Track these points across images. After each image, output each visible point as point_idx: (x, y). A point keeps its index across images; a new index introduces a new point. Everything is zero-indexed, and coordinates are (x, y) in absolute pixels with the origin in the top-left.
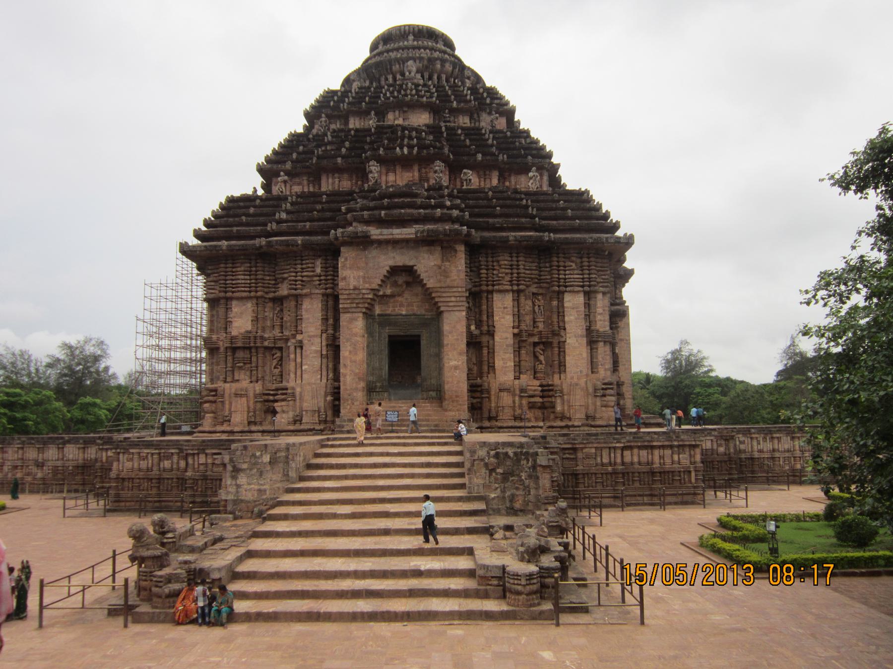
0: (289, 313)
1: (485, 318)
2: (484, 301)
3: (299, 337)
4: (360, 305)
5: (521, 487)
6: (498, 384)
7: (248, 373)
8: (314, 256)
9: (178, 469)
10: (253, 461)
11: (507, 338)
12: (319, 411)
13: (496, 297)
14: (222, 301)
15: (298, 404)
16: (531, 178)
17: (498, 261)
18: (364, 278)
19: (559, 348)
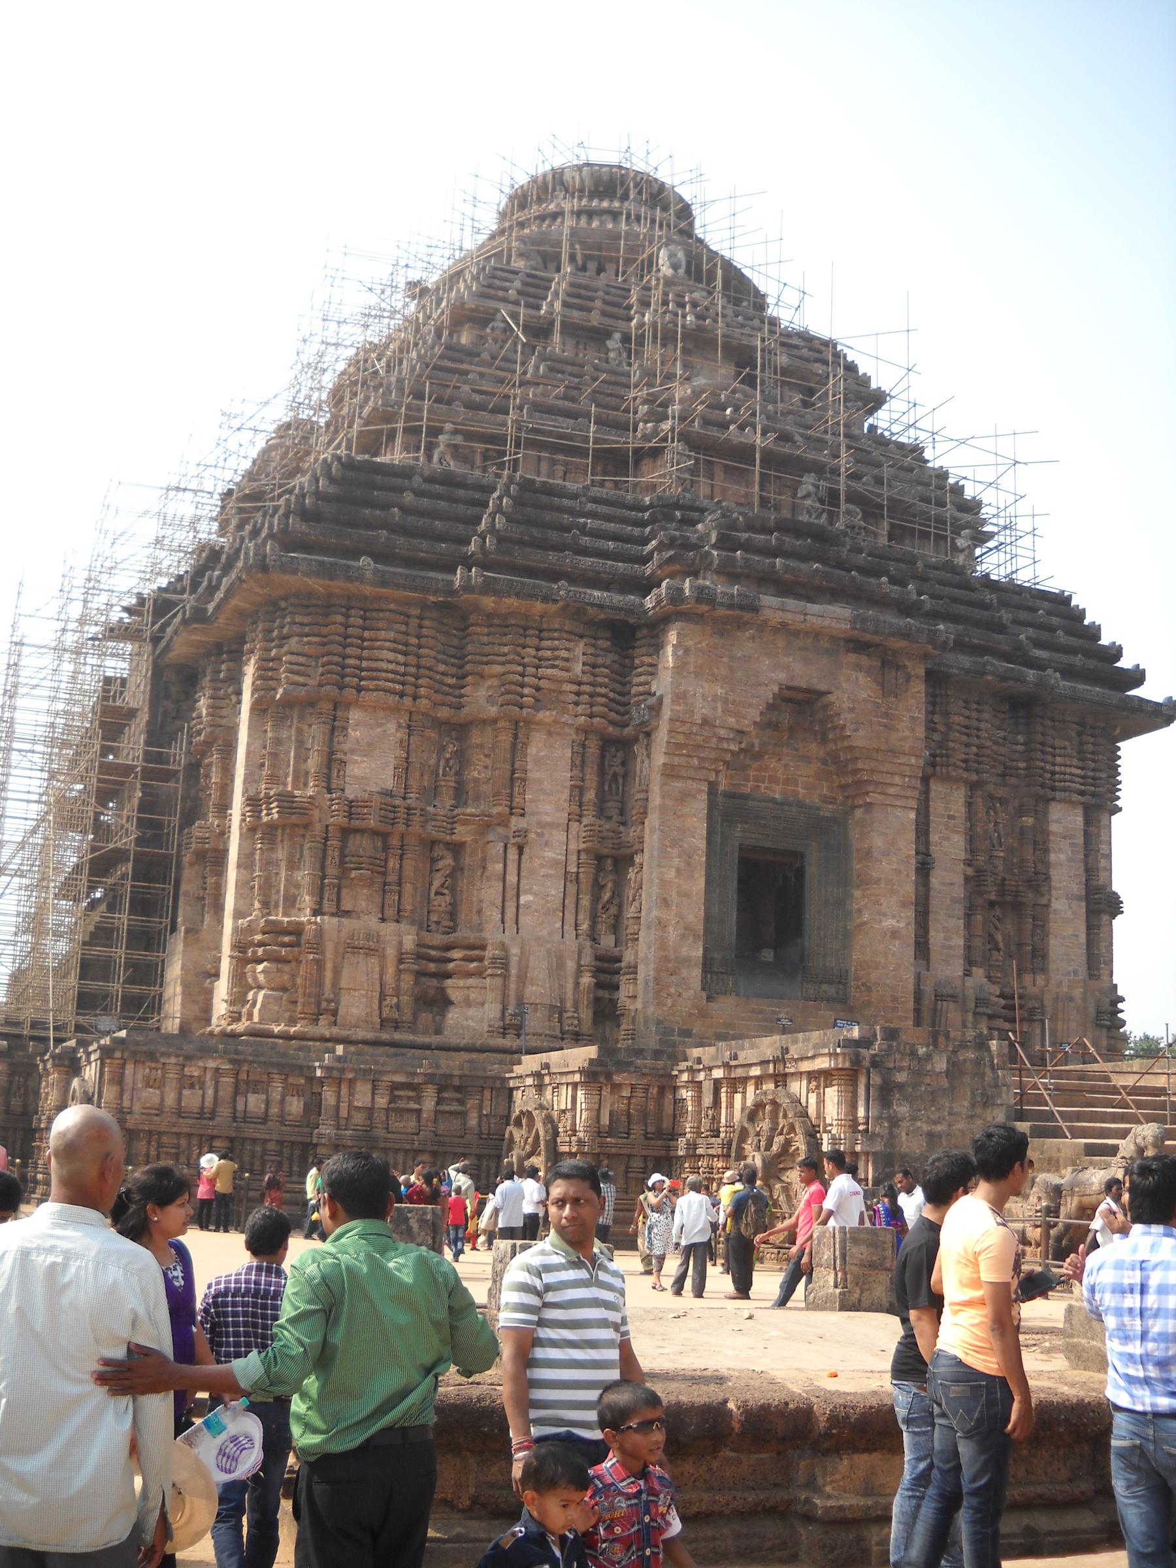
0: (488, 762)
7: (377, 898)
8: (570, 632)
9: (282, 1119)
12: (561, 1011)
13: (936, 788)
15: (513, 986)
16: (962, 551)
17: (946, 714)
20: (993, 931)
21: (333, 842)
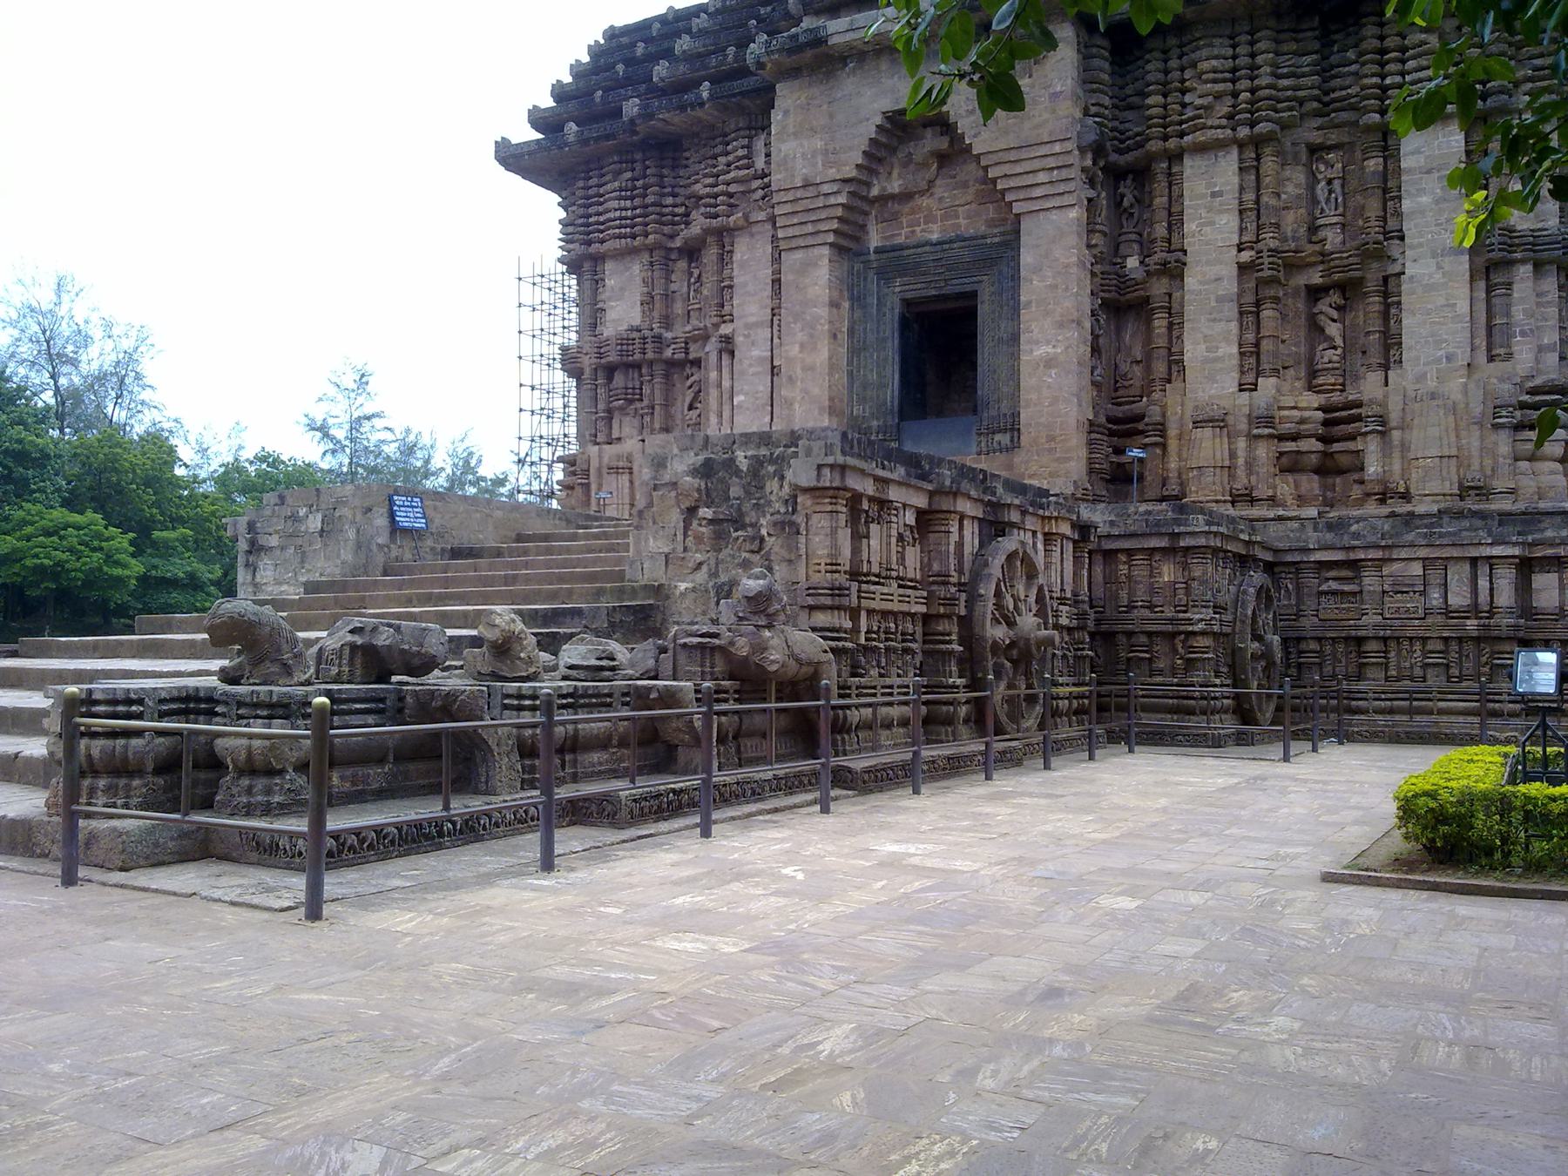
1: (1161, 230)
2: (1160, 186)
3: (725, 329)
4: (824, 227)
5: (756, 558)
6: (1190, 406)
7: (636, 422)
8: (749, 128)
11: (1216, 280)
13: (1192, 167)
14: (587, 266)
17: (1194, 65)
19: (1386, 295)
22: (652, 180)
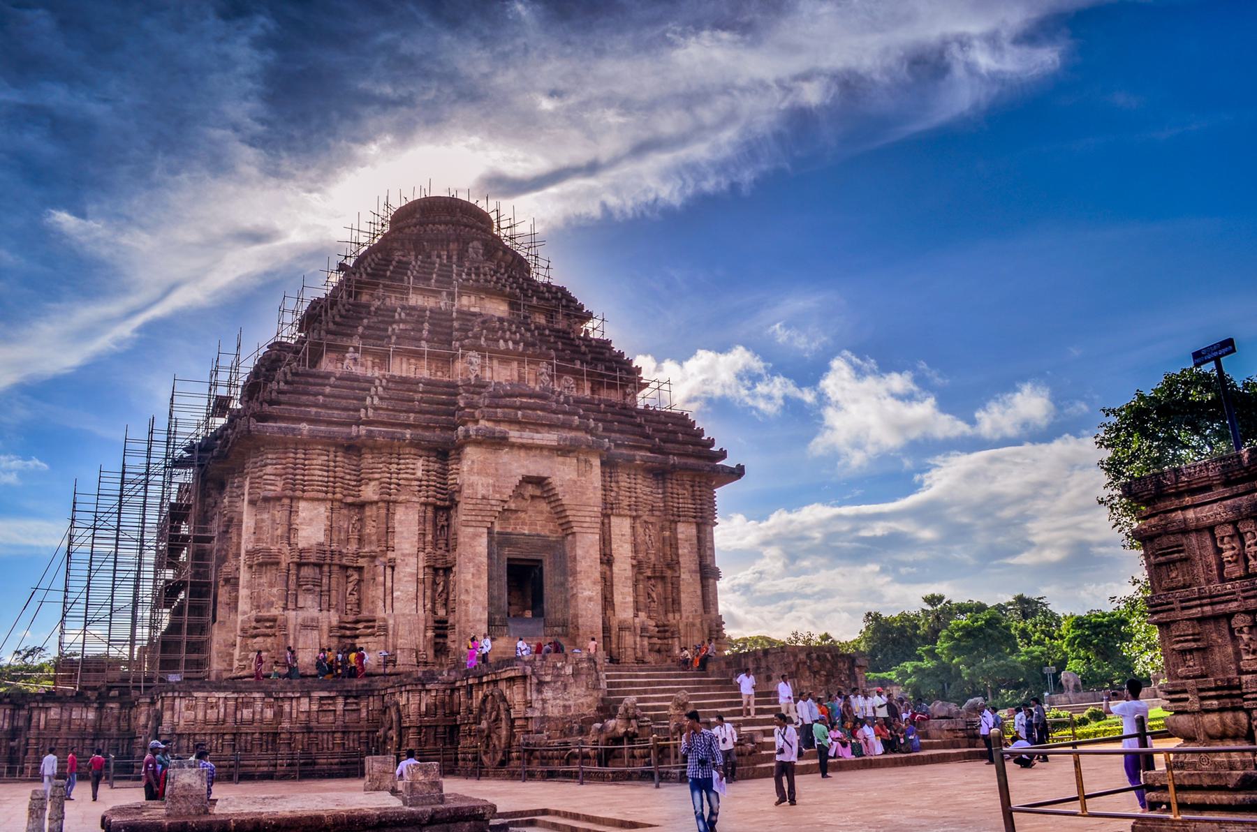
0: (374, 524)
3: (390, 555)
4: (486, 519)
7: (318, 599)
10: (555, 672)
12: (417, 652)
15: (390, 640)
17: (617, 482)
18: (494, 486)
20: (650, 592)
21: (293, 572)
22: (341, 464)
